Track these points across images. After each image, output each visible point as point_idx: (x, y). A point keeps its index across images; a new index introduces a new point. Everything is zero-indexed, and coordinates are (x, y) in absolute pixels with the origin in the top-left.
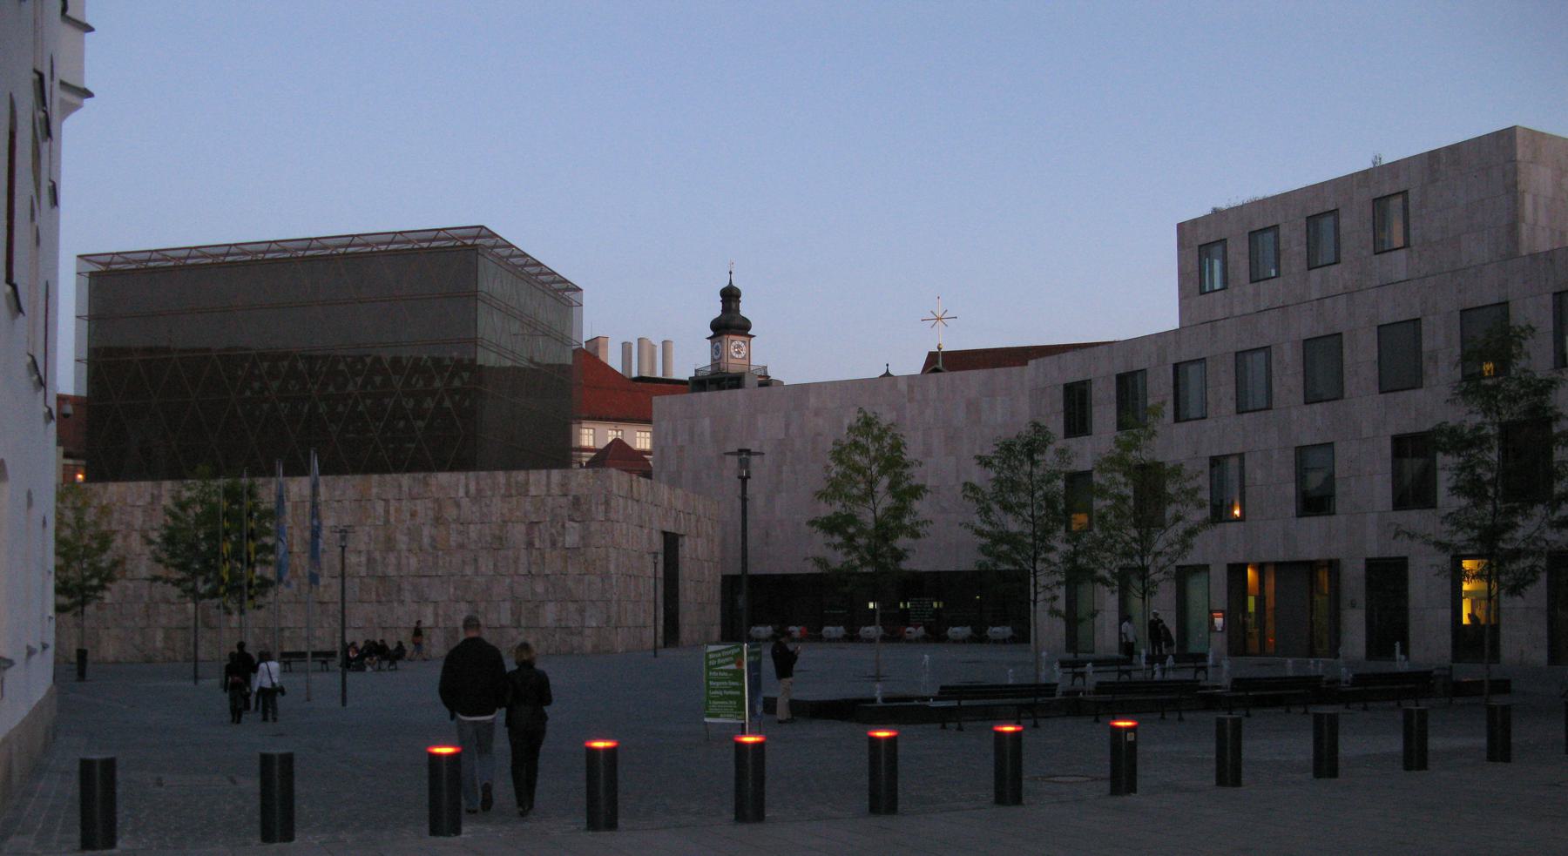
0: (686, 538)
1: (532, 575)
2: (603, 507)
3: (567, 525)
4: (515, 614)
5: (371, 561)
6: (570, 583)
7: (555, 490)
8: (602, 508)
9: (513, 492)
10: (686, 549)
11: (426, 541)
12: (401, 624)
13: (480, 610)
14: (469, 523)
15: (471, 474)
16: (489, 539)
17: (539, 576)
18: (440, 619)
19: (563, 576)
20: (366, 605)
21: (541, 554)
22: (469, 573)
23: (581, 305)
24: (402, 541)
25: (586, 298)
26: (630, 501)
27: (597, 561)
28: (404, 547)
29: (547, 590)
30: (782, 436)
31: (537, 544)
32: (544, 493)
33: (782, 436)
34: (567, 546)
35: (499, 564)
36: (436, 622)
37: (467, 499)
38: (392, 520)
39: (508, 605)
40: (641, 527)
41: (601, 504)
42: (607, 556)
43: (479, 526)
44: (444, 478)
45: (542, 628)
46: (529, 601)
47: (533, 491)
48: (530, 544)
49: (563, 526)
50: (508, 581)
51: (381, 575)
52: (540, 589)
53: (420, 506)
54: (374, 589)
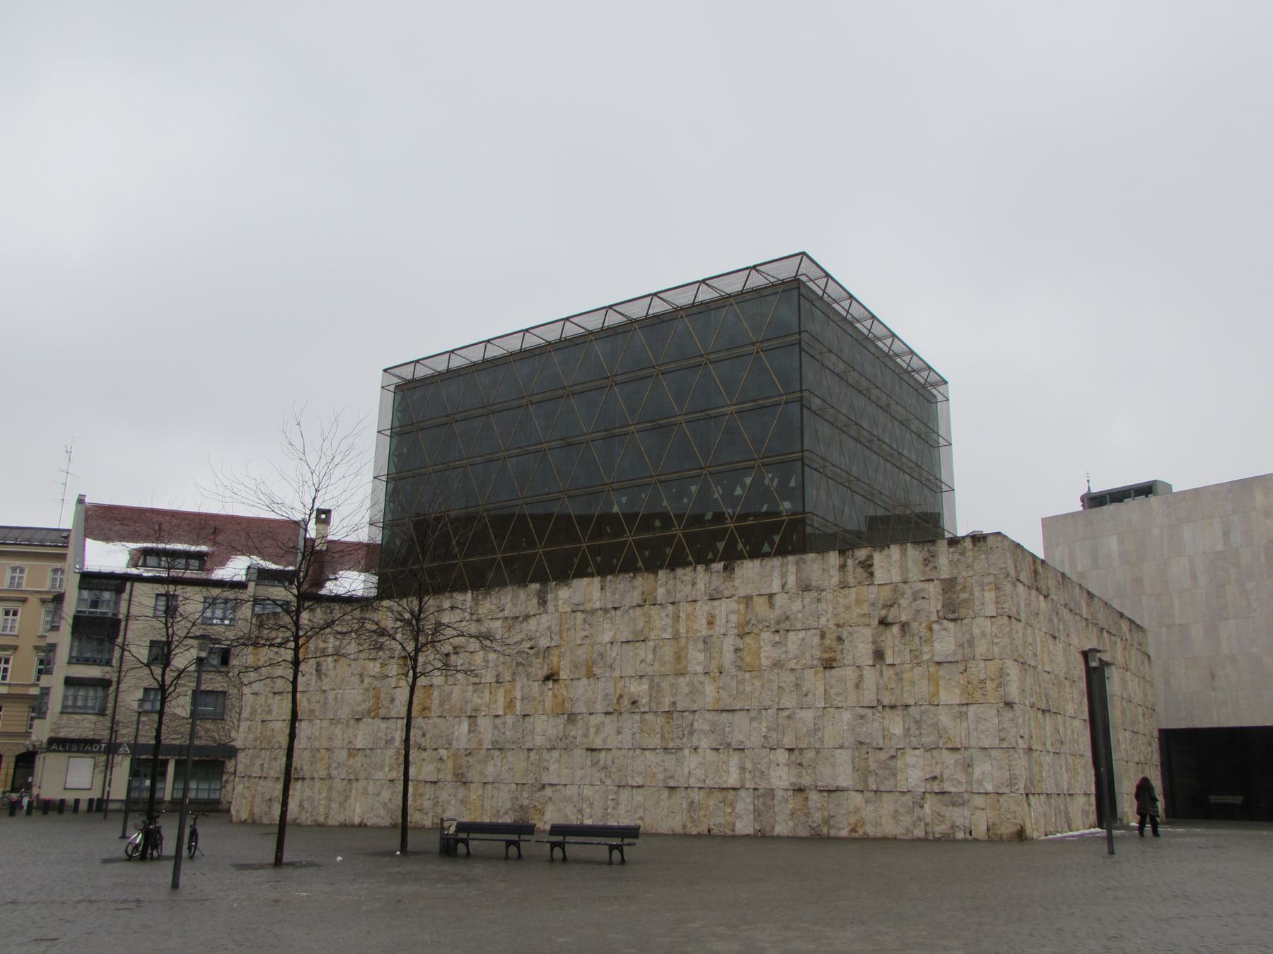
0: (1113, 667)
1: (883, 707)
2: (993, 594)
3: (935, 627)
4: (863, 772)
5: (655, 688)
6: (945, 719)
7: (915, 573)
8: (990, 596)
9: (851, 580)
10: (1115, 684)
11: (728, 656)
12: (693, 782)
13: (805, 763)
14: (788, 631)
15: (791, 558)
16: (818, 653)
17: (893, 707)
18: (748, 776)
19: (932, 708)
20: (647, 753)
21: (897, 674)
22: (787, 705)
23: (951, 444)
24: (696, 659)
25: (953, 390)
26: (1034, 592)
27: (988, 681)
28: (700, 669)
29: (907, 731)
30: (1220, 547)
31: (889, 661)
32: (896, 578)
33: (1220, 547)
34: (937, 659)
35: (833, 691)
36: (742, 780)
37: (786, 596)
38: (682, 631)
39: (844, 757)
40: (1055, 638)
41: (990, 590)
42: (1002, 673)
43: (802, 634)
44: (749, 570)
45: (903, 793)
46: (881, 749)
47: (880, 576)
48: (879, 655)
49: (930, 629)
50: (847, 716)
51: (667, 709)
52: (897, 728)
53: (723, 608)
54: (658, 730)
